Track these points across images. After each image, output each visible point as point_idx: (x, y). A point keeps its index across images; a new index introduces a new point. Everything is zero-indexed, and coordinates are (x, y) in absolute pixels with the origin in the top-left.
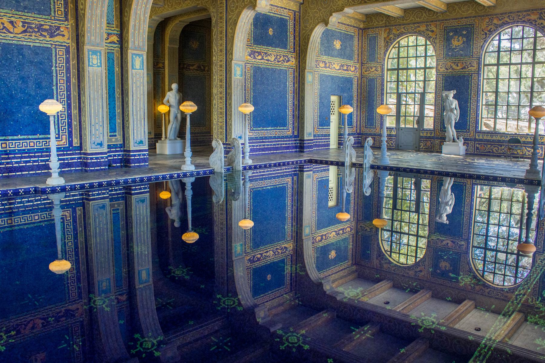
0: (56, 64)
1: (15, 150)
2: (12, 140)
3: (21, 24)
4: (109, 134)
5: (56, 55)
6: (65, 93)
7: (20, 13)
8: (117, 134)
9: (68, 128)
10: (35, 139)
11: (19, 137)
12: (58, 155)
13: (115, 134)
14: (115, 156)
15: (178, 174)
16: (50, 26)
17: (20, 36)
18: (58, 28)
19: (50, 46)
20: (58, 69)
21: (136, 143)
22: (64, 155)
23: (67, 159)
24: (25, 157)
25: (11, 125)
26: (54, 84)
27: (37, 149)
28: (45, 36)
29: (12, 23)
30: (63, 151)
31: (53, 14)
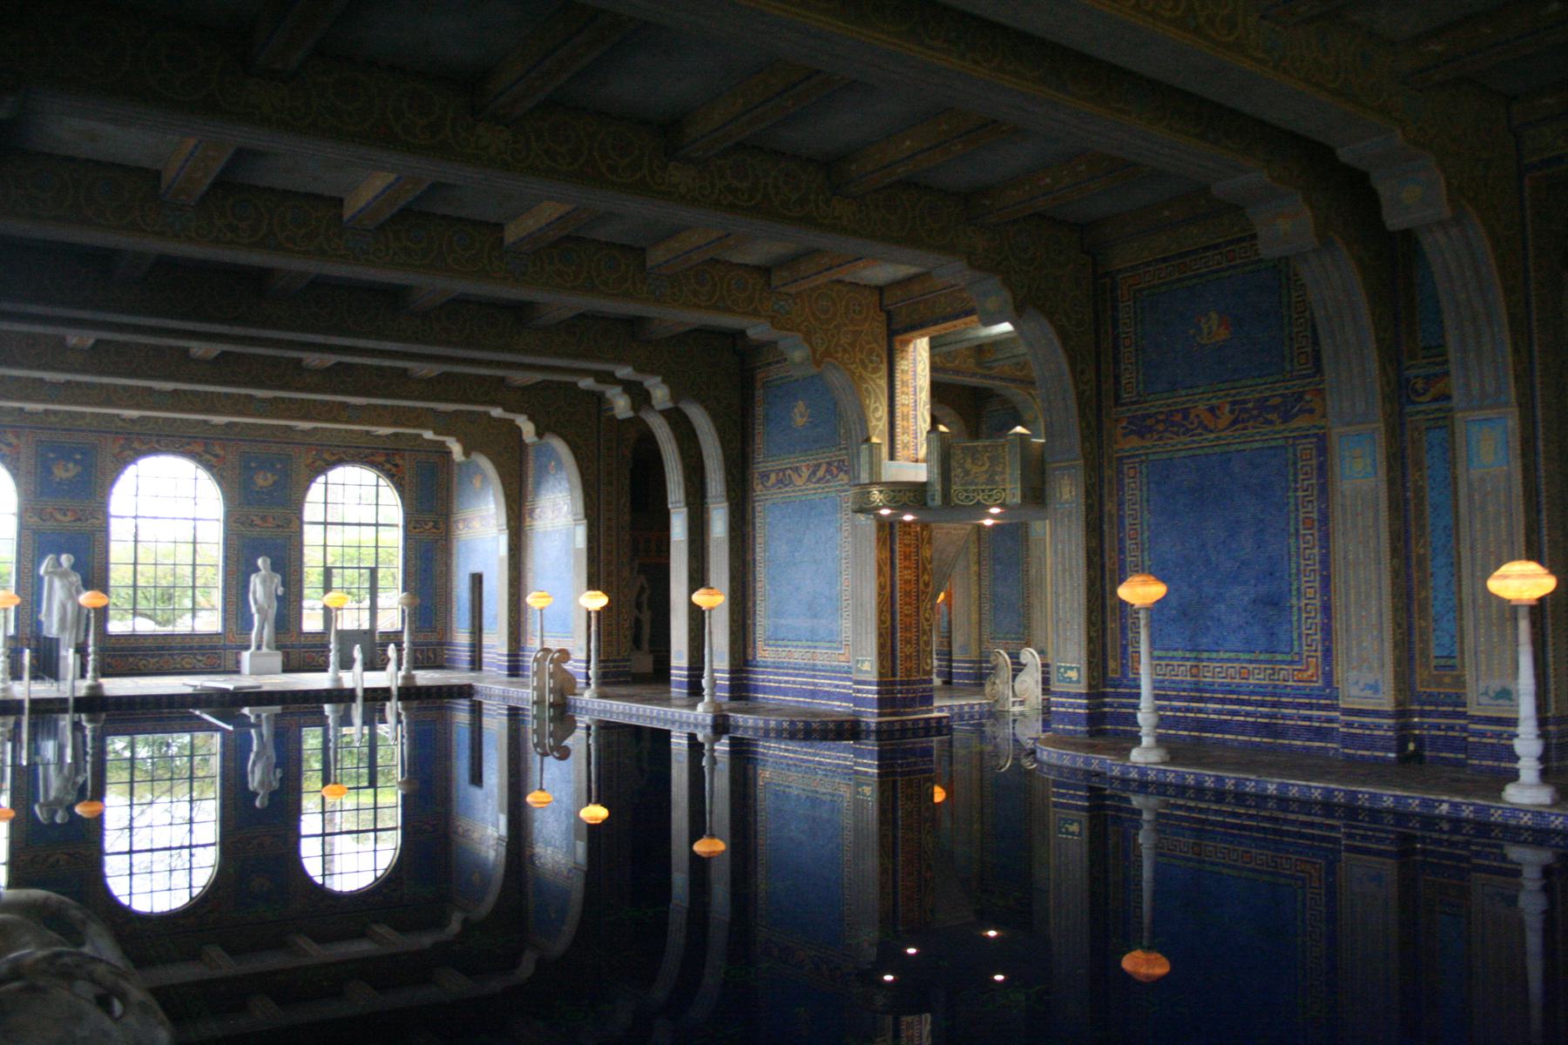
0: (1296, 482)
1: (1212, 684)
2: (1209, 659)
3: (1227, 408)
4: (1434, 662)
5: (1295, 463)
6: (1316, 551)
7: (1226, 385)
8: (1456, 662)
9: (1324, 640)
10: (1250, 662)
11: (1222, 655)
12: (1157, 697)
13: (1450, 662)
14: (1451, 728)
15: (1452, 804)
16: (1282, 395)
17: (1228, 433)
18: (1300, 397)
19: (1281, 442)
20: (1300, 493)
21: (1486, 693)
22: (1310, 706)
23: (1319, 718)
24: (1232, 702)
25: (1208, 628)
26: (1292, 530)
27: (1255, 685)
28: (1271, 423)
29: (1212, 410)
30: (1308, 696)
31: (1288, 368)
